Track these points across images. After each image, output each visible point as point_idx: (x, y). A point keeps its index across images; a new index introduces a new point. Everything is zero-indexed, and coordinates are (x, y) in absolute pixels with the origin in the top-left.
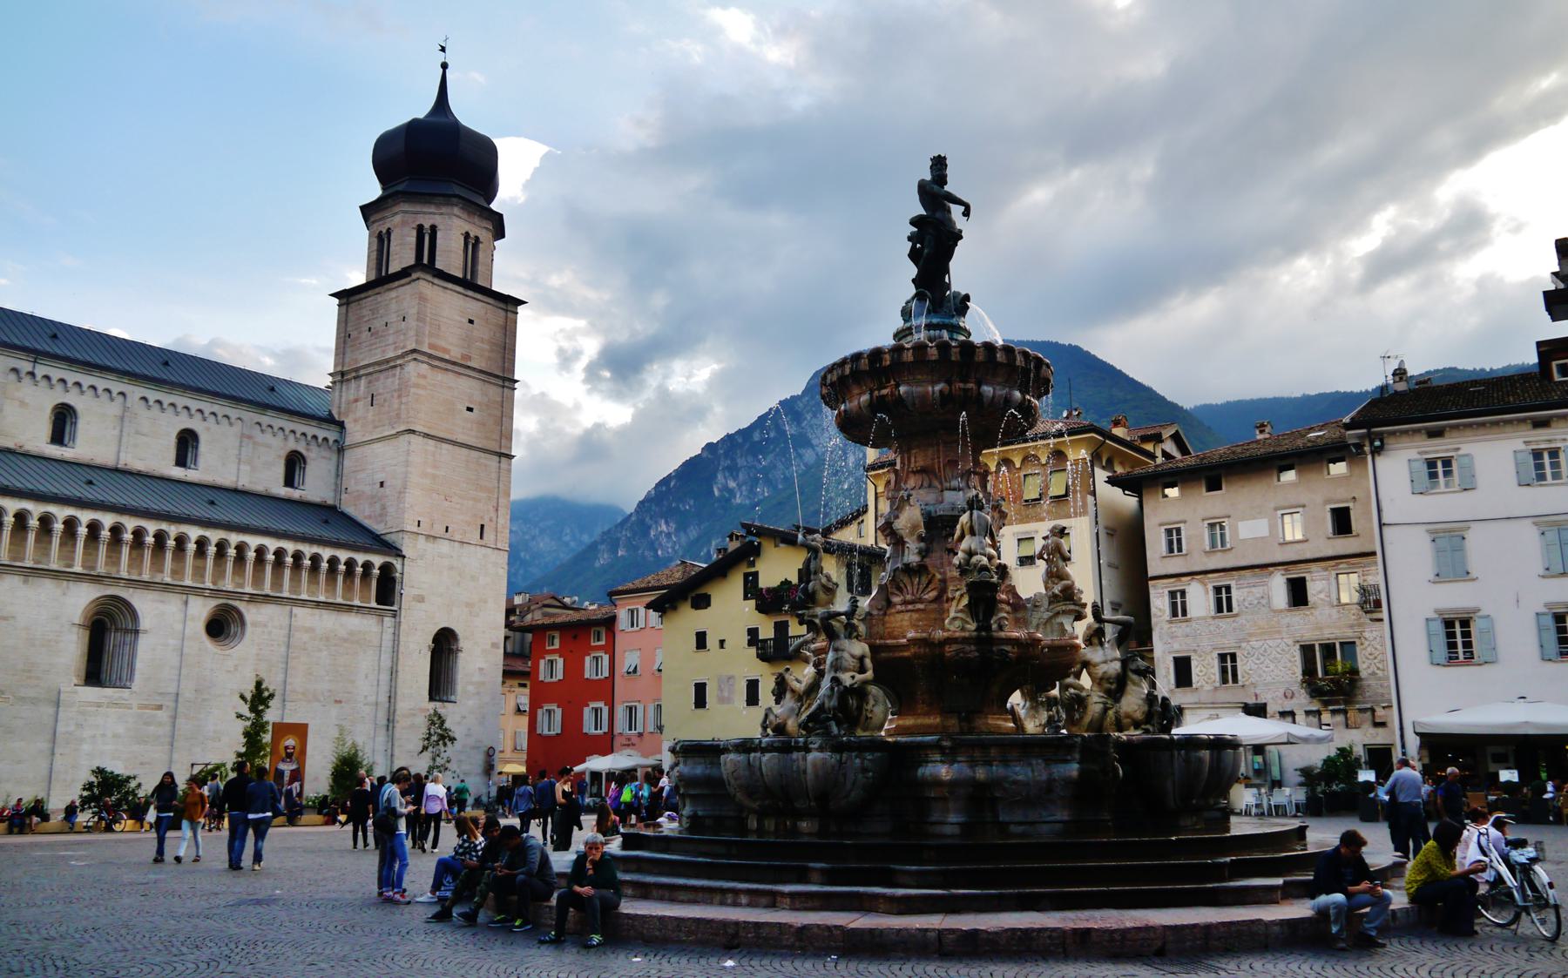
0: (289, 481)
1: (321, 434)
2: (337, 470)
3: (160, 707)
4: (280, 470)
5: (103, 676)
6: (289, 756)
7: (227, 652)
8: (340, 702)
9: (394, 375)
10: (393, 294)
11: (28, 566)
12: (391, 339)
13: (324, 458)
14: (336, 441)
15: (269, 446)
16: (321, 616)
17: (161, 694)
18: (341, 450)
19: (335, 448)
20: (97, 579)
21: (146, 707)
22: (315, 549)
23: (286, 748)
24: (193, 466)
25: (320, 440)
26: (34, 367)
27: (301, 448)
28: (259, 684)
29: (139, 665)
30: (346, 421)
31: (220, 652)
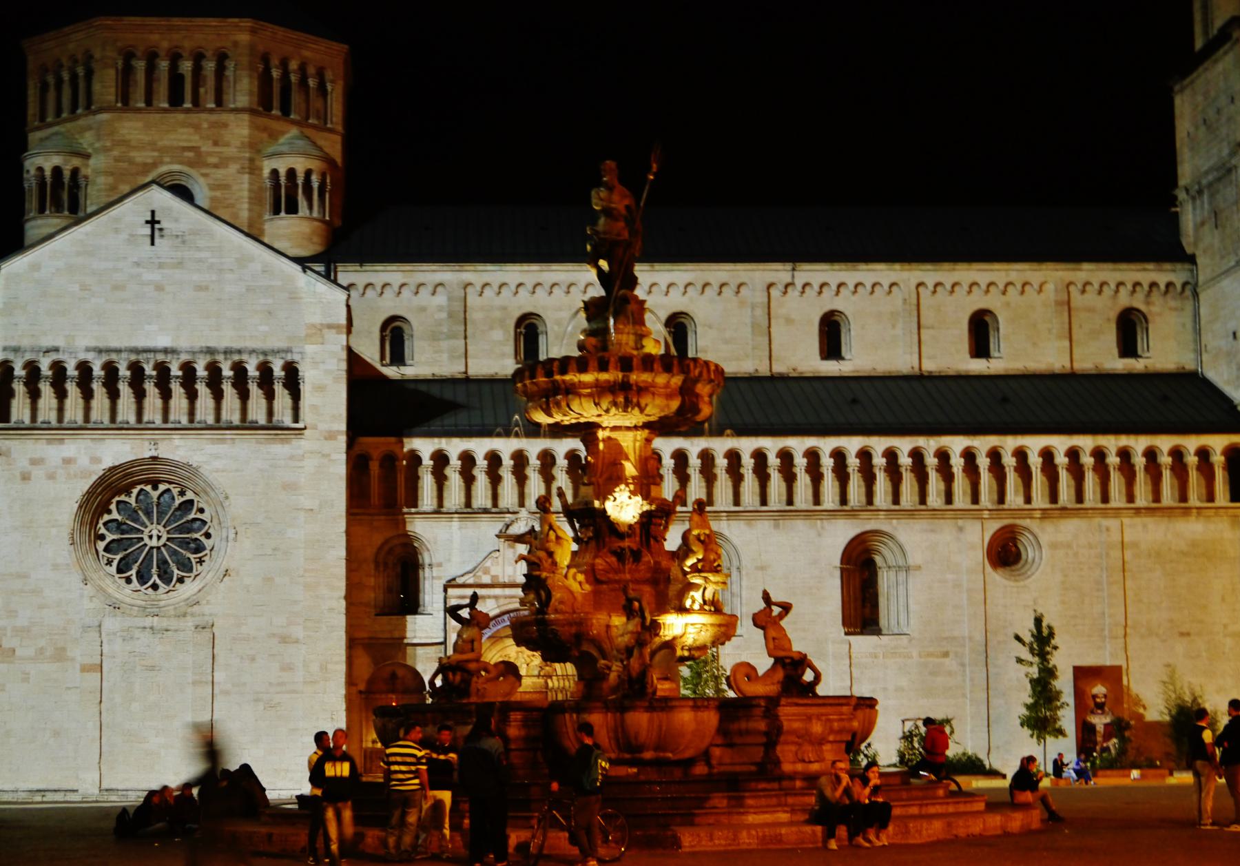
0: (1128, 347)
1: (1162, 278)
2: (1195, 322)
3: (946, 655)
4: (1110, 338)
5: (883, 622)
6: (1100, 706)
7: (1022, 583)
8: (1188, 634)
9: (1231, 182)
10: (1220, 67)
11: (775, 509)
12: (1224, 131)
13: (1171, 309)
14: (1185, 284)
15: (1091, 310)
16: (1145, 526)
17: (946, 638)
18: (1196, 295)
19: (1188, 292)
20: (853, 514)
21: (930, 655)
22: (1124, 441)
23: (1094, 697)
24: (996, 354)
25: (1163, 287)
26: (793, 277)
27: (1138, 302)
28: (1038, 621)
29: (912, 607)
30: (1198, 253)
31: (1012, 584)
